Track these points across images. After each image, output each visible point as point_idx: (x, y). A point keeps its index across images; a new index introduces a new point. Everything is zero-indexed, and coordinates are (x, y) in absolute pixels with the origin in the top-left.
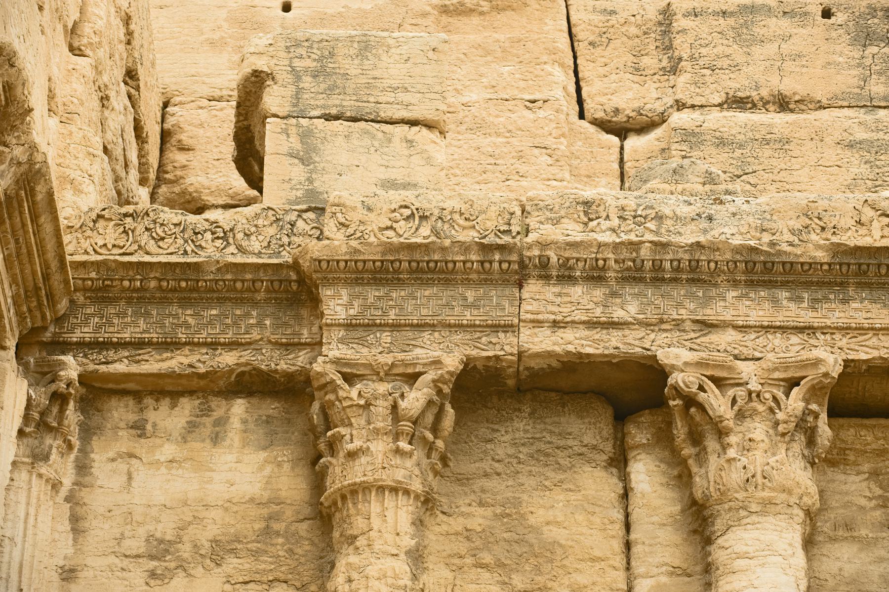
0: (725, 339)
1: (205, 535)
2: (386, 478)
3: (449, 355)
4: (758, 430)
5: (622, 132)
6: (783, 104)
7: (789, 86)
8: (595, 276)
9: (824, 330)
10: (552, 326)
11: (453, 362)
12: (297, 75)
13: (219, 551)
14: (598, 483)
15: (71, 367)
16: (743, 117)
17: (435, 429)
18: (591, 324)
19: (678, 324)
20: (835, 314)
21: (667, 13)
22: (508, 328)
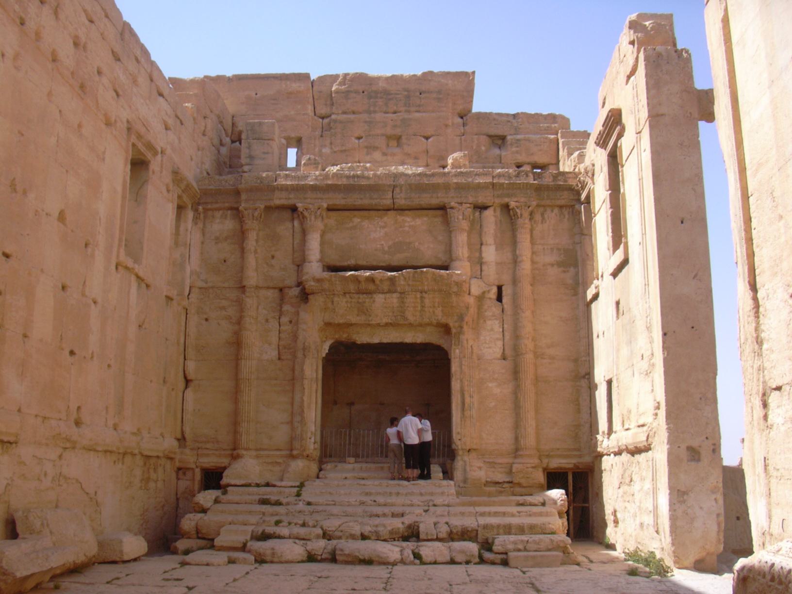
5: (323, 118)
6: (354, 113)
10: (279, 200)
11: (262, 207)
13: (226, 239)
14: (289, 225)
15: (200, 208)
16: (345, 116)
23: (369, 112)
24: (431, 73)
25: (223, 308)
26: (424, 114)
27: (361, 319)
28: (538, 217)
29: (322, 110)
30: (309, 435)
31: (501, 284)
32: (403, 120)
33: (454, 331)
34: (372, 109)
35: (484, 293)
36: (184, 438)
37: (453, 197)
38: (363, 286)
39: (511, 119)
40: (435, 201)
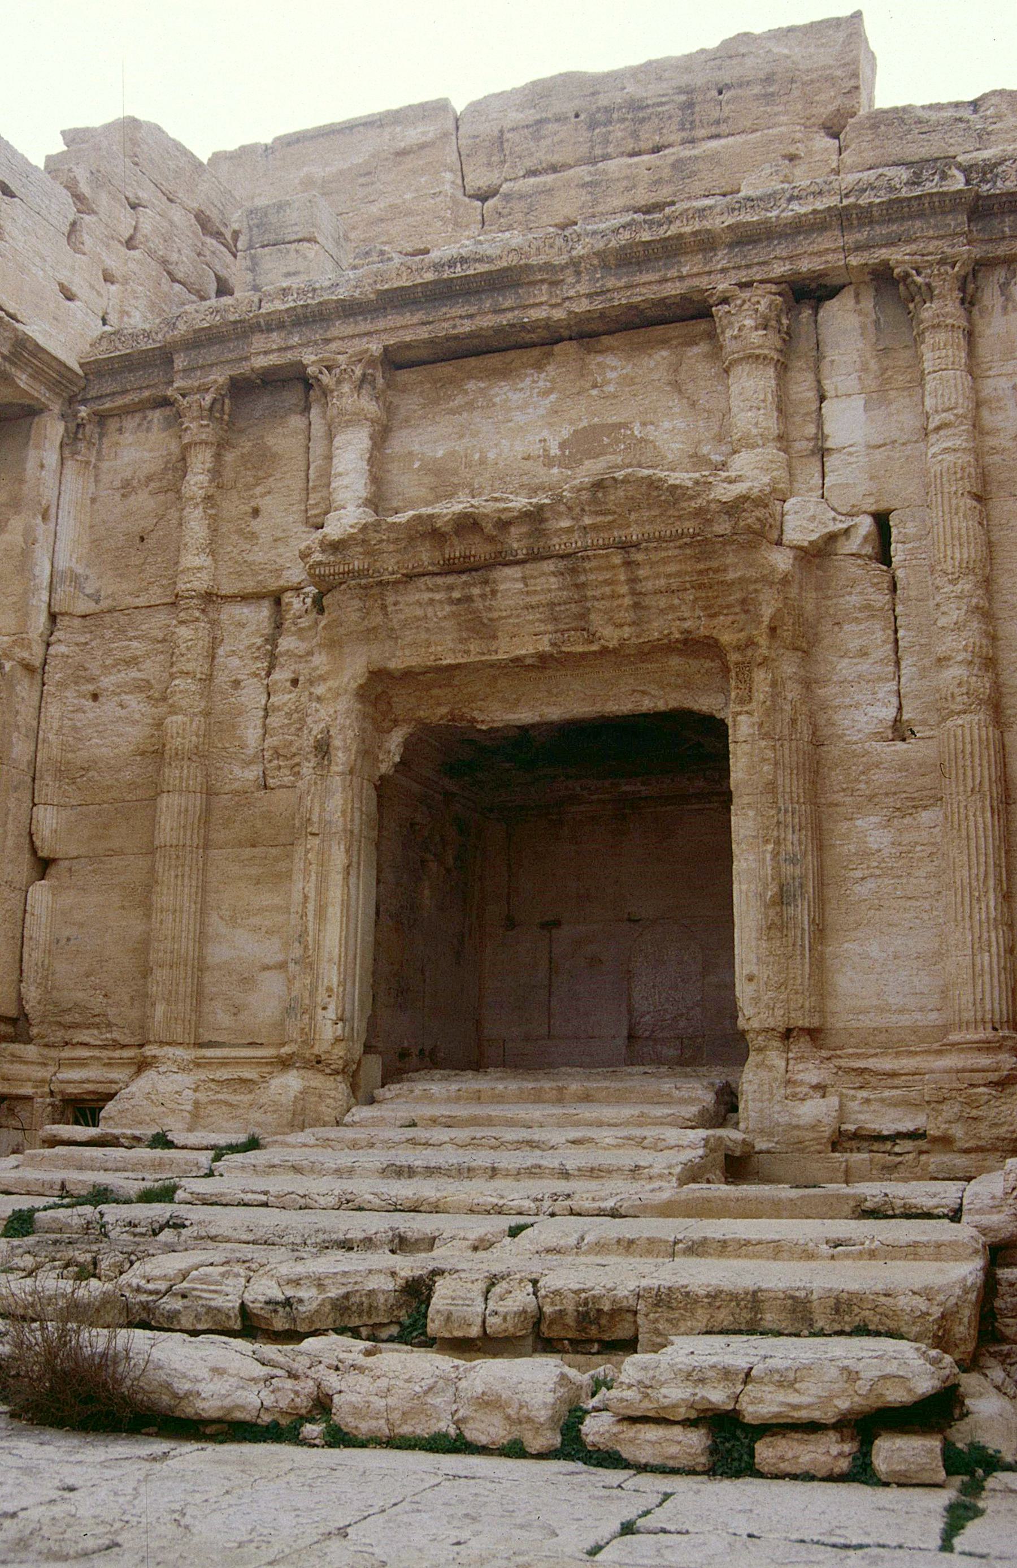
0: (334, 346)
1: (141, 475)
2: (197, 439)
3: (219, 377)
4: (346, 388)
5: (483, 198)
6: (554, 169)
7: (556, 158)
8: (281, 326)
9: (377, 332)
10: (264, 355)
12: (250, 229)
14: (296, 421)
16: (532, 180)
17: (222, 411)
18: (279, 350)
19: (316, 343)
20: (381, 324)
21: (501, 132)
22: (246, 359)
23: (593, 161)
24: (745, 37)
25: (133, 662)
26: (731, 139)
27: (475, 652)
28: (991, 296)
29: (479, 179)
30: (321, 996)
31: (883, 506)
32: (678, 165)
33: (734, 657)
34: (598, 151)
35: (832, 538)
36: (26, 1015)
37: (723, 270)
38: (457, 549)
39: (966, 114)
40: (673, 290)
